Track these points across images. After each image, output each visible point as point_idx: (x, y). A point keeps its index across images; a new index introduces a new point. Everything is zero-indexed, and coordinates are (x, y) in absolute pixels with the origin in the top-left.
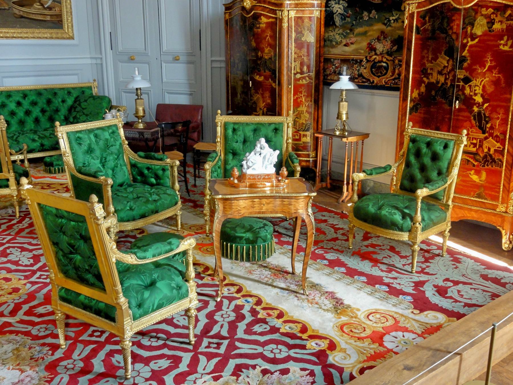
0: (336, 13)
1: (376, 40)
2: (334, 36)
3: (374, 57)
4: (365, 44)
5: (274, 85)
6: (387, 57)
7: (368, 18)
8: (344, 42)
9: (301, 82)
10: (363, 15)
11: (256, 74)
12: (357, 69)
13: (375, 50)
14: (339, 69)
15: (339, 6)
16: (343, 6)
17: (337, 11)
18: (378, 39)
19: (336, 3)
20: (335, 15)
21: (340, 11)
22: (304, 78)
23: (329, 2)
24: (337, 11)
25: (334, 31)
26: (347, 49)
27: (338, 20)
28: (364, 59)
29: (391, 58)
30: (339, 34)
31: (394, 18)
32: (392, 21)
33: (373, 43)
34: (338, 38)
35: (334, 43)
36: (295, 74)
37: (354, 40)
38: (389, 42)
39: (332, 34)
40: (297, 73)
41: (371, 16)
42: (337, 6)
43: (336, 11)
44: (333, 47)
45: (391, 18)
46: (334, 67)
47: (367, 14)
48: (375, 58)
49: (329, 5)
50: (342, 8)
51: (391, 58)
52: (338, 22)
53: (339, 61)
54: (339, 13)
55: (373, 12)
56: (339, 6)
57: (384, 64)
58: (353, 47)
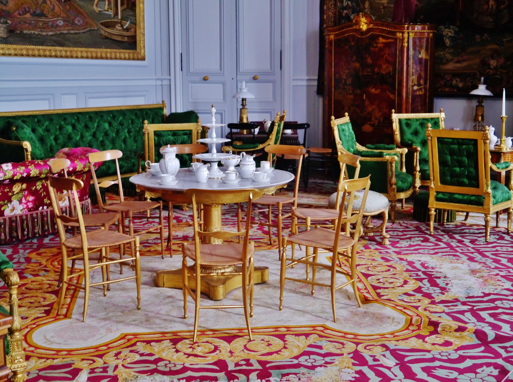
0: (446, 36)
1: (490, 57)
2: (444, 54)
3: (488, 71)
4: (477, 61)
5: (392, 96)
6: (501, 70)
7: (480, 40)
8: (456, 59)
9: (418, 93)
10: (476, 37)
11: (371, 88)
12: (471, 81)
13: (489, 65)
14: (451, 82)
15: (449, 30)
16: (454, 30)
17: (447, 34)
18: (492, 57)
19: (445, 28)
20: (445, 38)
21: (450, 34)
22: (420, 89)
23: (439, 27)
24: (447, 34)
25: (445, 51)
26: (458, 65)
27: (448, 42)
28: (478, 73)
29: (505, 71)
30: (450, 53)
31: (507, 39)
32: (505, 42)
33: (486, 60)
34: (448, 56)
35: (444, 61)
36: (413, 86)
37: (466, 57)
38: (503, 59)
39: (442, 53)
40: (415, 85)
41: (483, 38)
42: (447, 30)
43: (446, 34)
44: (444, 64)
45: (504, 40)
46: (444, 80)
47: (479, 37)
48: (489, 72)
49: (438, 30)
50: (453, 32)
51: (505, 71)
52: (449, 43)
53: (451, 76)
54: (450, 36)
55: (486, 35)
56: (449, 30)
57: (498, 76)
58: (465, 64)
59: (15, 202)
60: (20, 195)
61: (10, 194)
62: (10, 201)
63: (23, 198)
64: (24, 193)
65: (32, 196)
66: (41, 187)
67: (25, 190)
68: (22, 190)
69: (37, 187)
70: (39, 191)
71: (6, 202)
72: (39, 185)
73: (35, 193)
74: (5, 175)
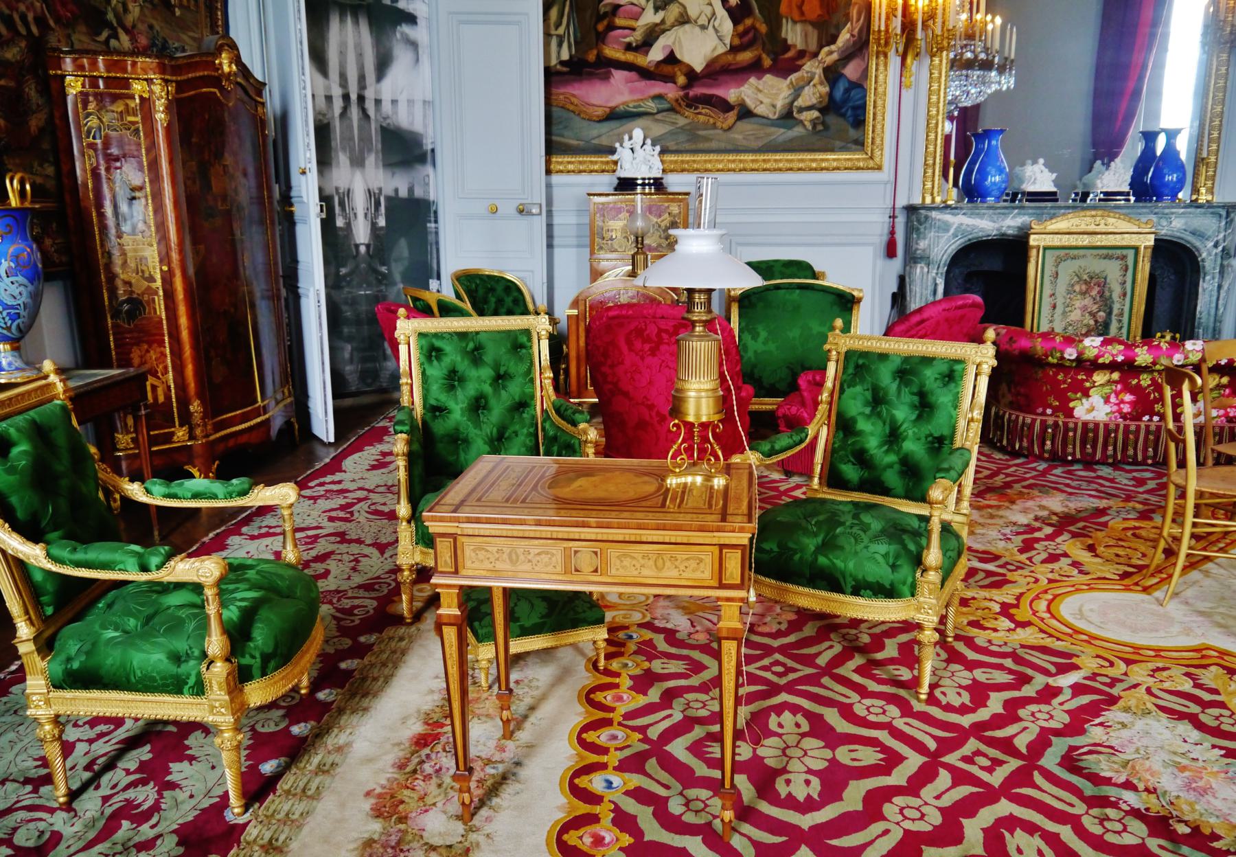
59: (1096, 398)
60: (1107, 390)
61: (1088, 384)
62: (1086, 394)
63: (1113, 396)
64: (1114, 387)
65: (1131, 394)
66: (1150, 382)
67: (1116, 382)
68: (1110, 382)
69: (1142, 383)
70: (1146, 388)
71: (1079, 395)
72: (1145, 380)
73: (1137, 390)
74: (1186, 357)
